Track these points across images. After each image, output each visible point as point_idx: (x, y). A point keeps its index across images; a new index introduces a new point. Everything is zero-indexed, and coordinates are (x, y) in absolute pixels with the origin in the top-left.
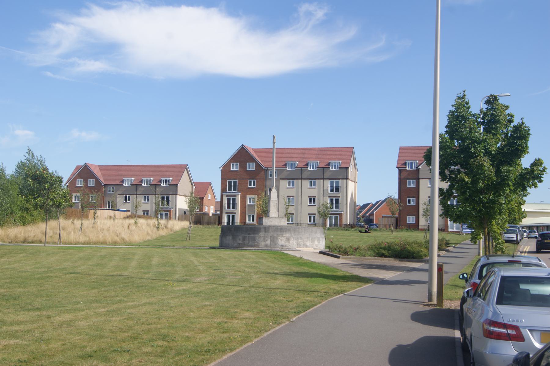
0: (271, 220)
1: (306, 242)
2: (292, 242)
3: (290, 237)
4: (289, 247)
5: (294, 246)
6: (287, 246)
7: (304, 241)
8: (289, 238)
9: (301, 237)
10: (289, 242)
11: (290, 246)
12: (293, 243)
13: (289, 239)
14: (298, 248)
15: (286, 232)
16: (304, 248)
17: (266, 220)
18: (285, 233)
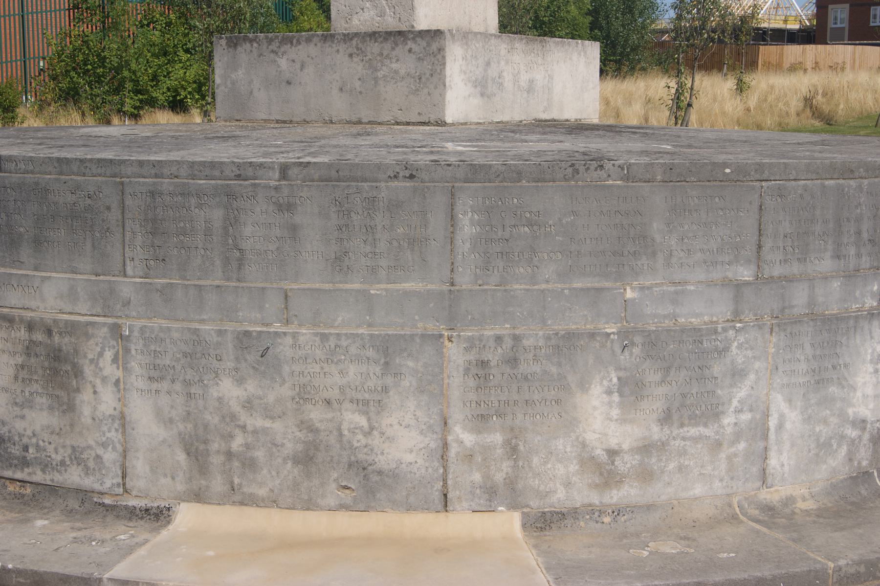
0: (283, 62)
1: (352, 418)
2: (108, 402)
3: (72, 328)
4: (74, 477)
5: (139, 466)
6: (45, 466)
7: (304, 395)
8: (64, 342)
9: (244, 339)
10: (70, 408)
11: (77, 457)
12: (123, 421)
13: (56, 356)
14: (198, 497)
15: (38, 243)
16: (309, 505)
17: (240, 74)
18: (25, 253)
